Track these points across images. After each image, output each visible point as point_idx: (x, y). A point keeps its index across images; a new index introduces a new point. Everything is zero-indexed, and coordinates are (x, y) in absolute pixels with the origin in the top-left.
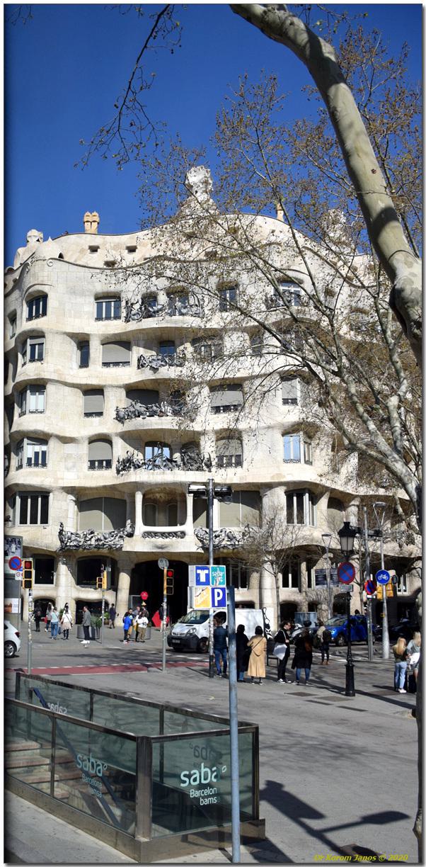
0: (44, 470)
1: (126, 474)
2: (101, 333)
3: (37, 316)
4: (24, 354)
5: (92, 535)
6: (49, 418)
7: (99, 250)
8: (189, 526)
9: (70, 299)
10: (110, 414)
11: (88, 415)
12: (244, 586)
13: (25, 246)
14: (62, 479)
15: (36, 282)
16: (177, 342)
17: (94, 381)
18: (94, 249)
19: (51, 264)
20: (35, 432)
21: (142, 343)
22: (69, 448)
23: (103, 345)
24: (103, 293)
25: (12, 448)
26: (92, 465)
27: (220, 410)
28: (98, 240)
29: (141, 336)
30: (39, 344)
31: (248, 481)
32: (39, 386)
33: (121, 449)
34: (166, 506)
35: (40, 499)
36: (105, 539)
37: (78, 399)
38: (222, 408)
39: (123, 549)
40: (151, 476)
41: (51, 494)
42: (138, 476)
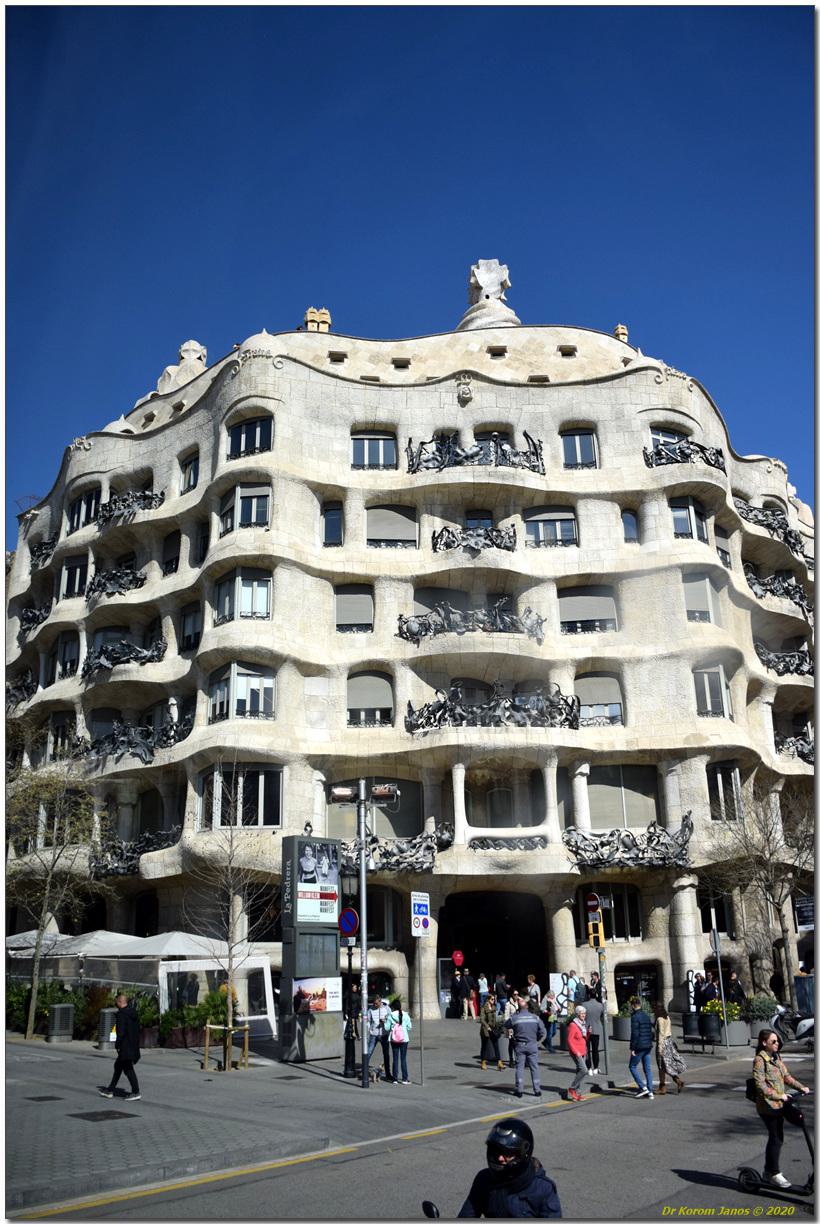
0: (270, 722)
1: (435, 732)
2: (368, 487)
3: (251, 450)
4: (227, 514)
5: (374, 845)
6: (279, 628)
7: (345, 360)
8: (552, 826)
9: (310, 426)
10: (387, 625)
11: (342, 628)
12: (635, 934)
13: (178, 364)
14: (305, 741)
15: (253, 393)
16: (499, 512)
17: (358, 569)
18: (337, 358)
19: (279, 366)
20: (256, 652)
21: (439, 509)
22: (314, 685)
23: (367, 509)
24: (367, 423)
25: (200, 683)
26: (354, 718)
27: (577, 628)
28: (342, 344)
29: (438, 497)
30: (258, 497)
31: (642, 746)
32: (259, 570)
33: (414, 691)
34: (508, 789)
35: (262, 778)
36: (402, 851)
37: (325, 602)
38: (579, 625)
39: (436, 871)
40: (486, 736)
41: (286, 769)
42: (462, 736)
